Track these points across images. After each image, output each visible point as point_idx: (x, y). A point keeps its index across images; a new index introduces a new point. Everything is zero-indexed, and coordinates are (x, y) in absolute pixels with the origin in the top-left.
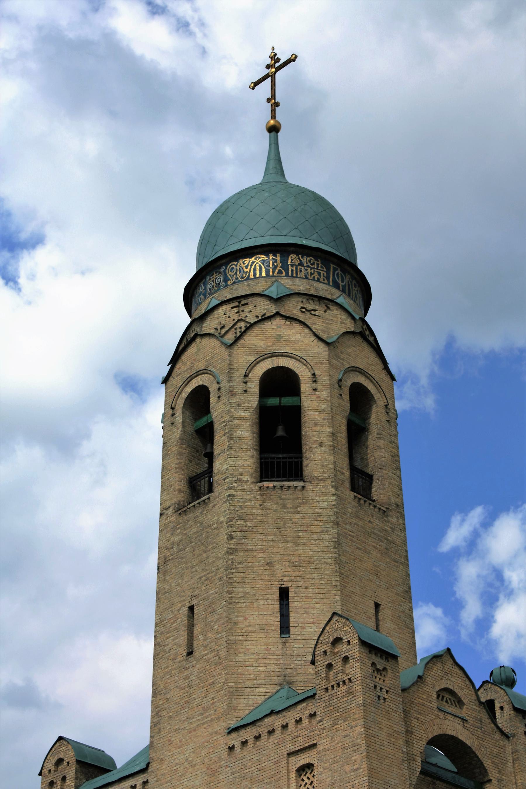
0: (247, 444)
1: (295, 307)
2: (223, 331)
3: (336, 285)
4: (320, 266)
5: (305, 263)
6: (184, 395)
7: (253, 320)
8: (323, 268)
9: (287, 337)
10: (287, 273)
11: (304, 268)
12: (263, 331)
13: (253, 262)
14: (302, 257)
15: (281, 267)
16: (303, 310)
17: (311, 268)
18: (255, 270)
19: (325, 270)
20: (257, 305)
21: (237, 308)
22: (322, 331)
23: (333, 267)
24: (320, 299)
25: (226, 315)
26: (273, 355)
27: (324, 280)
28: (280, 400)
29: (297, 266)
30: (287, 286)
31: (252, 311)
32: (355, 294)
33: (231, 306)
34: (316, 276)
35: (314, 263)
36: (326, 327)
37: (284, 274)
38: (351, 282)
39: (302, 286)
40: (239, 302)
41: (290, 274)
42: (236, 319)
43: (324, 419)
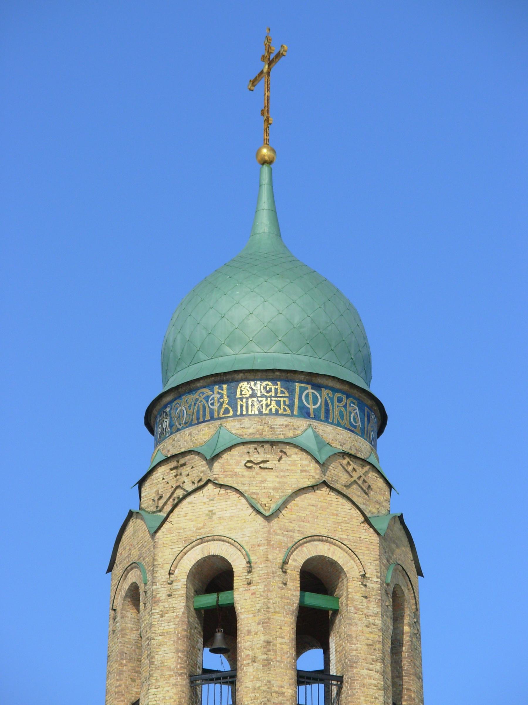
0: (170, 669)
1: (237, 464)
2: (161, 503)
3: (305, 413)
4: (279, 391)
5: (259, 391)
6: (123, 593)
7: (189, 487)
8: (285, 393)
9: (221, 513)
10: (235, 411)
11: (258, 400)
12: (193, 508)
13: (197, 400)
14: (255, 384)
15: (228, 404)
16: (249, 465)
17: (267, 397)
18: (198, 411)
19: (287, 395)
20: (194, 466)
21: (175, 471)
22: (274, 489)
23: (301, 387)
24: (272, 443)
25: (164, 480)
26: (202, 540)
27: (285, 410)
28: (218, 598)
29: (247, 398)
30: (233, 432)
31: (189, 473)
32: (341, 412)
33: (170, 467)
34: (274, 407)
35: (271, 389)
36: (280, 483)
37: (231, 414)
38: (332, 399)
39: (252, 428)
40: (178, 462)
41: (239, 413)
42: (174, 486)
43: (259, 624)
